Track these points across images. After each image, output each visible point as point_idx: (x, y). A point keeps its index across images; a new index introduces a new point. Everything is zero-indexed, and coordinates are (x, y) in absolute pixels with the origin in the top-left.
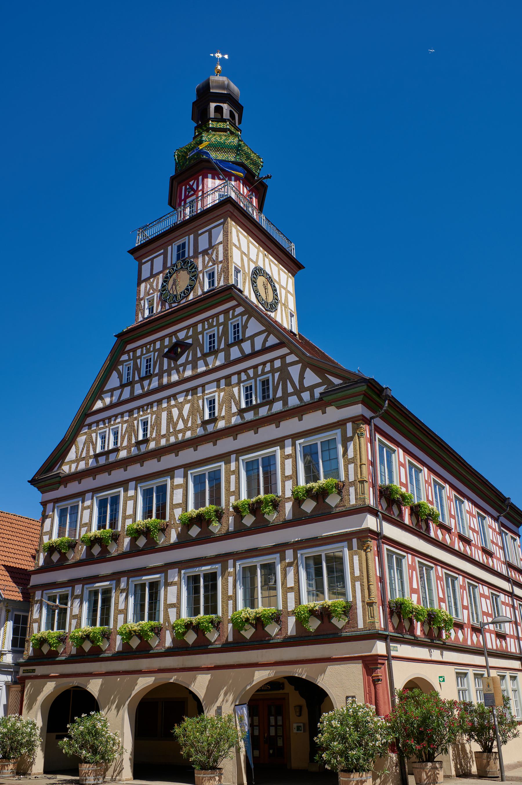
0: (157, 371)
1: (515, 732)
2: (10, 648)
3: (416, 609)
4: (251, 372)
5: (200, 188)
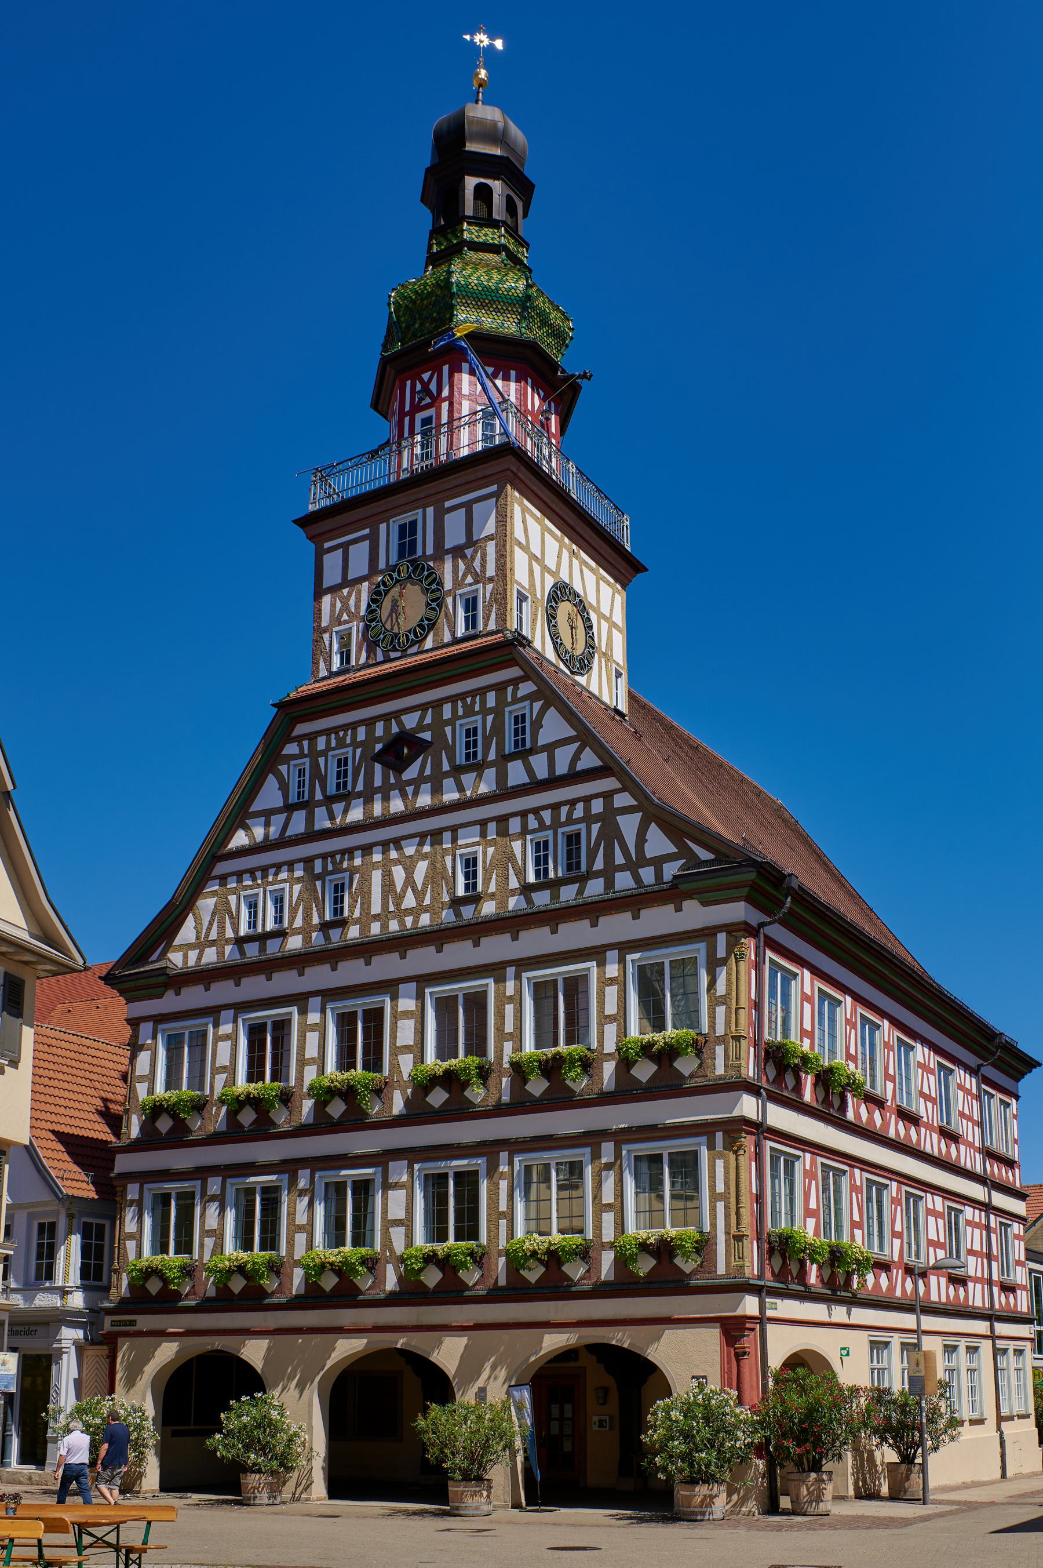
0: (360, 787)
2: (79, 1282)
3: (811, 1245)
4: (547, 816)
5: (445, 393)
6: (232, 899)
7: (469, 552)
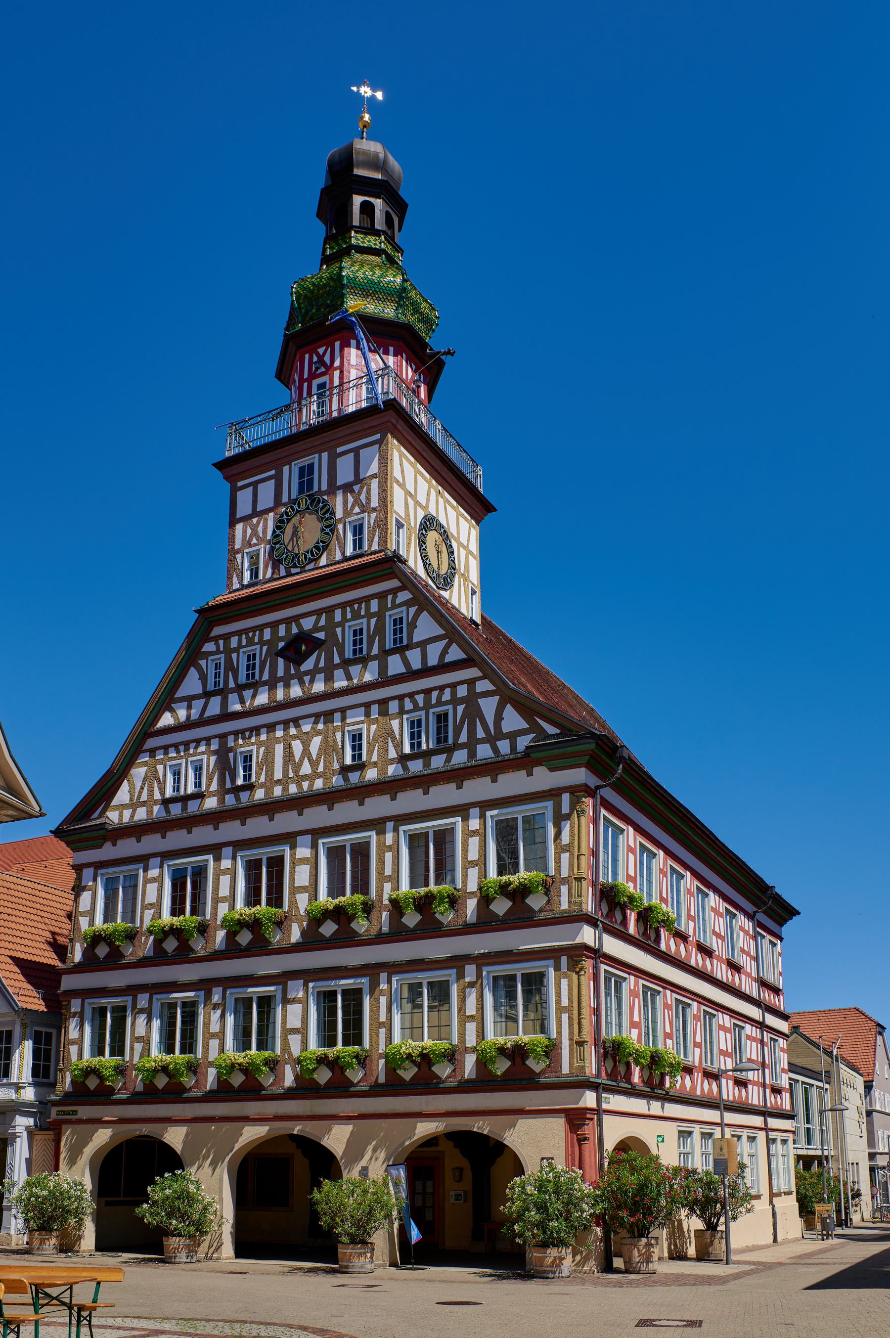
0: (266, 677)
1: (749, 1207)
2: (30, 1079)
3: (637, 1050)
4: (420, 699)
5: (337, 363)
6: (160, 768)
7: (356, 488)
